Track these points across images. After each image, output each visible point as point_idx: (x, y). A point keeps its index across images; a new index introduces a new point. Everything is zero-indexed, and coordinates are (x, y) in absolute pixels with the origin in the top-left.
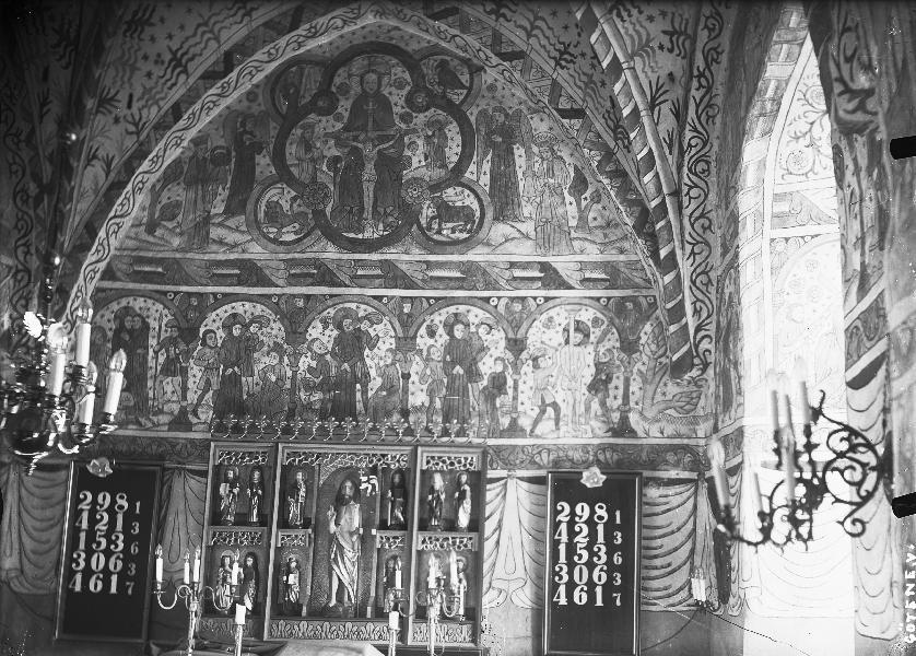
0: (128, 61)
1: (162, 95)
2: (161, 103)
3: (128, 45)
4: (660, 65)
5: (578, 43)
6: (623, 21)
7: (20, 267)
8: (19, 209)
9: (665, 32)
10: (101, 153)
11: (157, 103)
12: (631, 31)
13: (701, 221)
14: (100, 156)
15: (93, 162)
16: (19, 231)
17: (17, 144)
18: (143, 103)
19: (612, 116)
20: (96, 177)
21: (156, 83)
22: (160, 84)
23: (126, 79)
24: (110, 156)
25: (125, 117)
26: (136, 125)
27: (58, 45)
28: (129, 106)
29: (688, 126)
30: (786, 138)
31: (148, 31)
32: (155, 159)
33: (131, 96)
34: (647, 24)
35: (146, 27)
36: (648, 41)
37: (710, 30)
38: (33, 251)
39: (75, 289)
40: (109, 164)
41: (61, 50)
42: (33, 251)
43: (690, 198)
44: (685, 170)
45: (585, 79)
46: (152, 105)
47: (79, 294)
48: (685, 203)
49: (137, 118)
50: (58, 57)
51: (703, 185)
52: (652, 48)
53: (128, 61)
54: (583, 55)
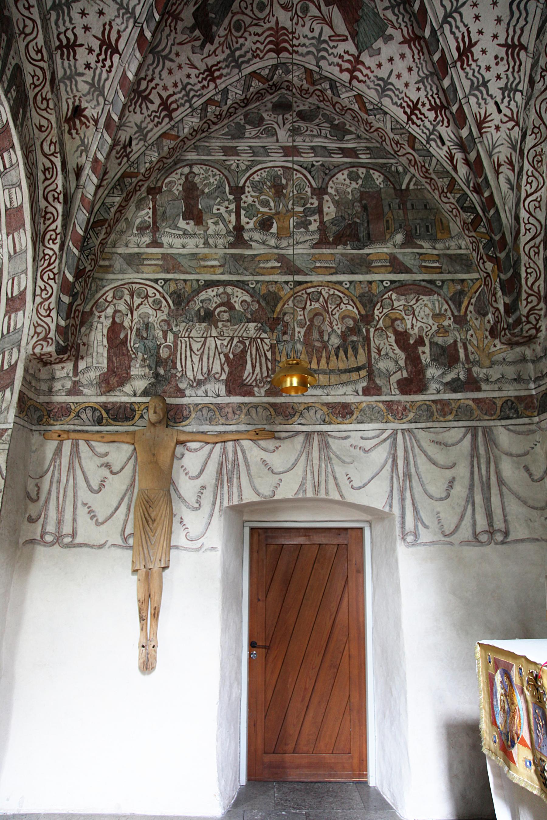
0: (478, 82)
1: (517, 80)
2: (520, 87)
3: (471, 73)
7: (485, 275)
8: (470, 237)
10: (503, 159)
11: (516, 90)
14: (503, 163)
15: (501, 169)
16: (475, 250)
17: (446, 197)
18: (507, 99)
20: (508, 180)
21: (507, 77)
22: (510, 76)
23: (485, 96)
24: (509, 157)
25: (501, 121)
26: (511, 119)
27: (437, 117)
28: (500, 111)
31: (476, 50)
32: (536, 130)
33: (496, 103)
35: (473, 49)
38: (485, 260)
39: (523, 269)
40: (511, 163)
41: (440, 118)
42: (485, 260)
46: (514, 94)
47: (529, 271)
49: (509, 114)
50: (441, 124)
53: (478, 82)
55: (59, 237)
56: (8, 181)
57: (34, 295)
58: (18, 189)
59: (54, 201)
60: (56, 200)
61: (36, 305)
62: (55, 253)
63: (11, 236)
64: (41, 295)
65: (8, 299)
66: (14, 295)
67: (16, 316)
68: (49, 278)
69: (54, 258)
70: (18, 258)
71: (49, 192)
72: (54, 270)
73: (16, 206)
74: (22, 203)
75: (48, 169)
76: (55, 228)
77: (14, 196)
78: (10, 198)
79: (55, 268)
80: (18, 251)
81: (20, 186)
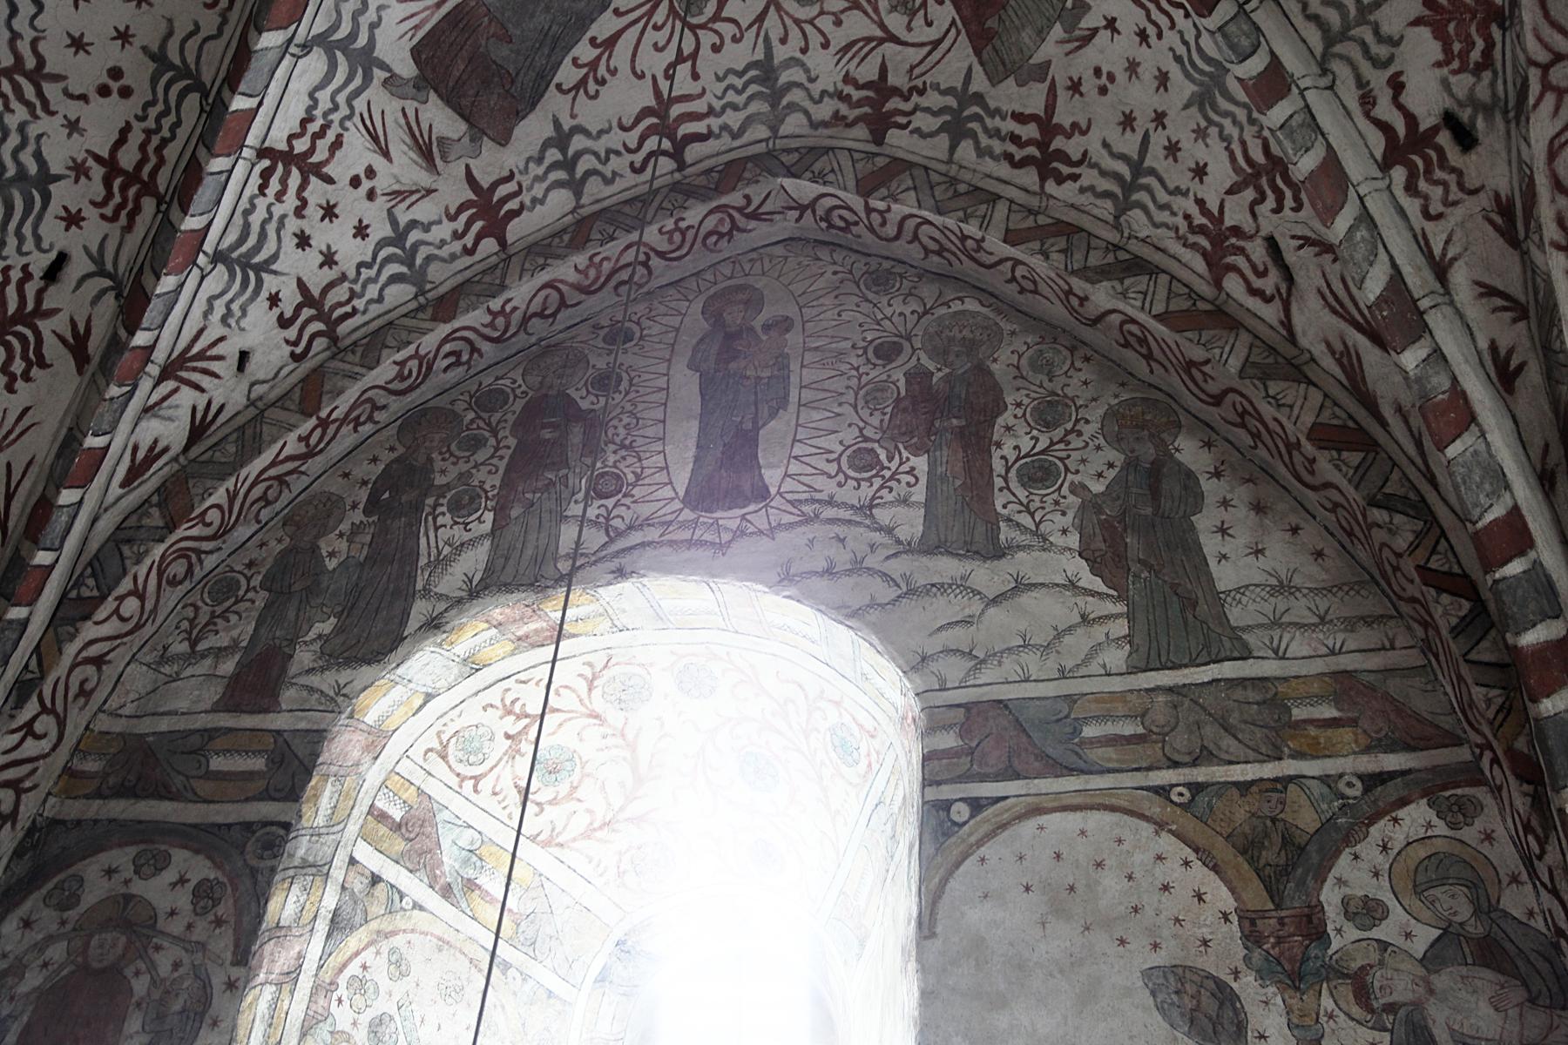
4: (243, 324)
5: (84, 98)
6: (262, 189)
9: (301, 284)
12: (256, 219)
13: (90, 670)
19: (31, 289)
29: (230, 484)
30: (493, 696)
34: (289, 242)
36: (265, 266)
37: (401, 377)
43: (116, 611)
44: (158, 551)
45: (33, 168)
48: (101, 614)
51: (149, 606)
52: (259, 282)
54: (73, 126)
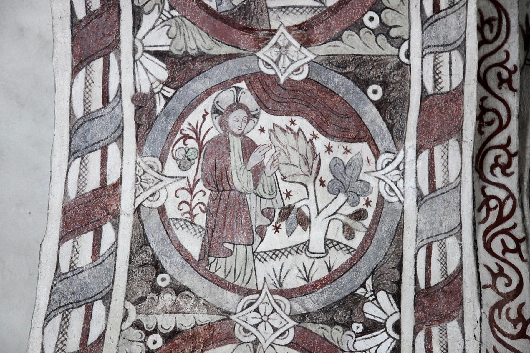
55: (515, 160)
56: (437, 37)
57: (480, 287)
58: (456, 55)
59: (500, 86)
60: (505, 85)
61: (487, 310)
62: (511, 195)
63: (425, 154)
64: (494, 287)
65: (418, 292)
66: (433, 283)
67: (444, 333)
68: (506, 250)
69: (509, 204)
70: (439, 201)
71: (490, 67)
72: (513, 232)
73: (446, 89)
74: (462, 83)
75: (490, 21)
76: (504, 142)
77: (444, 70)
78: (436, 73)
79: (515, 226)
80: (439, 185)
81: (462, 48)
